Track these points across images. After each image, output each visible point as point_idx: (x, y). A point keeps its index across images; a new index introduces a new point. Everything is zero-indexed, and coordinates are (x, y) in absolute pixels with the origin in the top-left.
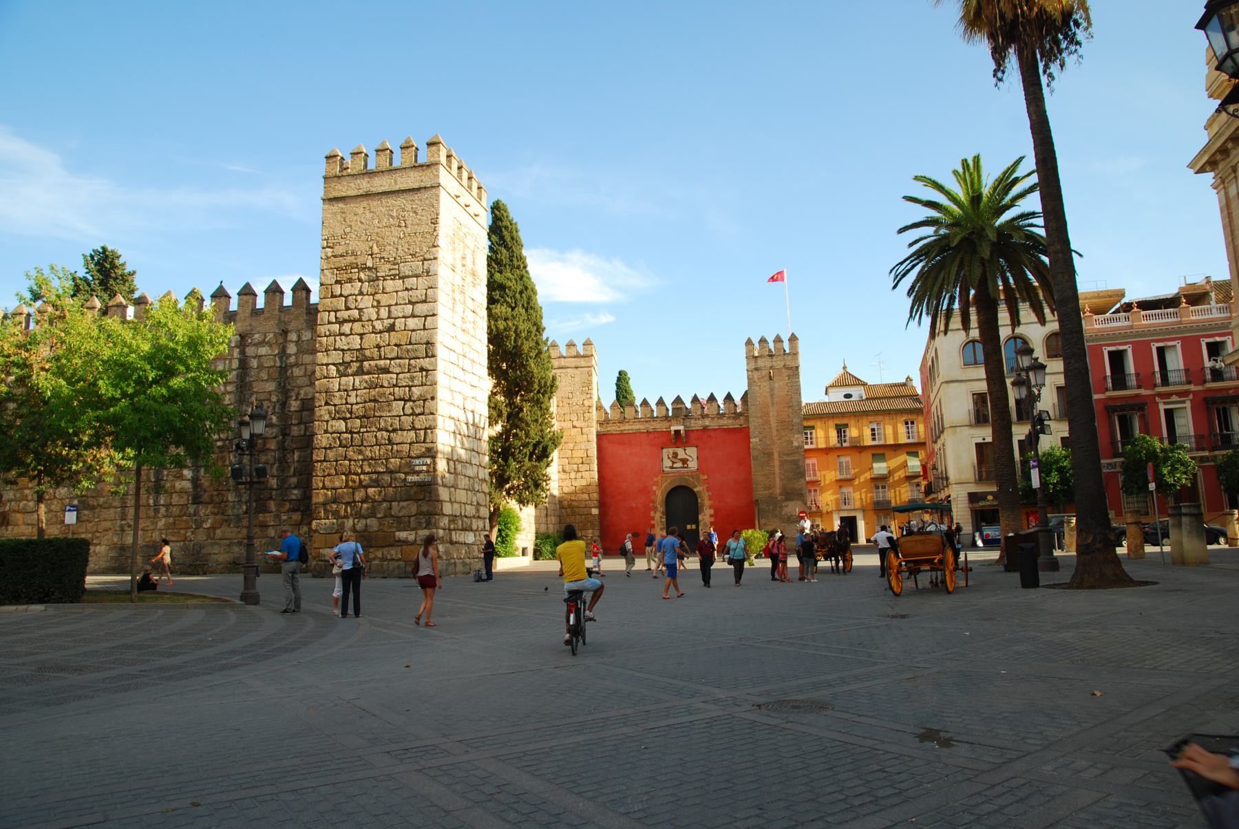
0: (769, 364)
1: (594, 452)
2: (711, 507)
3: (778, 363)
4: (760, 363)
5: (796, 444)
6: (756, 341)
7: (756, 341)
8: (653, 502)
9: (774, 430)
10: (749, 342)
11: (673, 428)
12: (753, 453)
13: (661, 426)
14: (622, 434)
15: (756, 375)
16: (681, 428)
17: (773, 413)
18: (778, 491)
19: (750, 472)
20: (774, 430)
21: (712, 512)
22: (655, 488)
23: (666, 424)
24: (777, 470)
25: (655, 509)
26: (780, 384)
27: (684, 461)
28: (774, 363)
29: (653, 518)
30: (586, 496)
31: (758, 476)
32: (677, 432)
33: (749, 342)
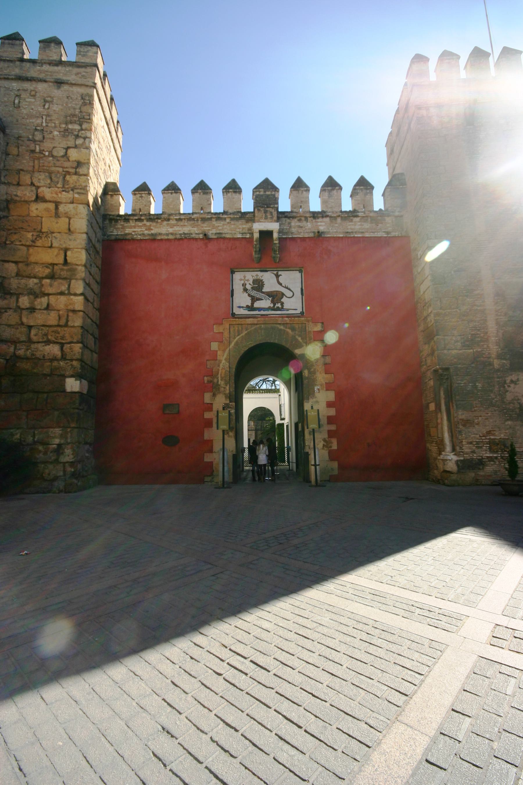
1: (79, 256)
2: (328, 387)
8: (212, 374)
14: (153, 239)
16: (274, 226)
18: (494, 349)
21: (331, 396)
22: (214, 346)
25: (214, 389)
27: (276, 297)
29: (209, 407)
30: (55, 350)
32: (266, 235)
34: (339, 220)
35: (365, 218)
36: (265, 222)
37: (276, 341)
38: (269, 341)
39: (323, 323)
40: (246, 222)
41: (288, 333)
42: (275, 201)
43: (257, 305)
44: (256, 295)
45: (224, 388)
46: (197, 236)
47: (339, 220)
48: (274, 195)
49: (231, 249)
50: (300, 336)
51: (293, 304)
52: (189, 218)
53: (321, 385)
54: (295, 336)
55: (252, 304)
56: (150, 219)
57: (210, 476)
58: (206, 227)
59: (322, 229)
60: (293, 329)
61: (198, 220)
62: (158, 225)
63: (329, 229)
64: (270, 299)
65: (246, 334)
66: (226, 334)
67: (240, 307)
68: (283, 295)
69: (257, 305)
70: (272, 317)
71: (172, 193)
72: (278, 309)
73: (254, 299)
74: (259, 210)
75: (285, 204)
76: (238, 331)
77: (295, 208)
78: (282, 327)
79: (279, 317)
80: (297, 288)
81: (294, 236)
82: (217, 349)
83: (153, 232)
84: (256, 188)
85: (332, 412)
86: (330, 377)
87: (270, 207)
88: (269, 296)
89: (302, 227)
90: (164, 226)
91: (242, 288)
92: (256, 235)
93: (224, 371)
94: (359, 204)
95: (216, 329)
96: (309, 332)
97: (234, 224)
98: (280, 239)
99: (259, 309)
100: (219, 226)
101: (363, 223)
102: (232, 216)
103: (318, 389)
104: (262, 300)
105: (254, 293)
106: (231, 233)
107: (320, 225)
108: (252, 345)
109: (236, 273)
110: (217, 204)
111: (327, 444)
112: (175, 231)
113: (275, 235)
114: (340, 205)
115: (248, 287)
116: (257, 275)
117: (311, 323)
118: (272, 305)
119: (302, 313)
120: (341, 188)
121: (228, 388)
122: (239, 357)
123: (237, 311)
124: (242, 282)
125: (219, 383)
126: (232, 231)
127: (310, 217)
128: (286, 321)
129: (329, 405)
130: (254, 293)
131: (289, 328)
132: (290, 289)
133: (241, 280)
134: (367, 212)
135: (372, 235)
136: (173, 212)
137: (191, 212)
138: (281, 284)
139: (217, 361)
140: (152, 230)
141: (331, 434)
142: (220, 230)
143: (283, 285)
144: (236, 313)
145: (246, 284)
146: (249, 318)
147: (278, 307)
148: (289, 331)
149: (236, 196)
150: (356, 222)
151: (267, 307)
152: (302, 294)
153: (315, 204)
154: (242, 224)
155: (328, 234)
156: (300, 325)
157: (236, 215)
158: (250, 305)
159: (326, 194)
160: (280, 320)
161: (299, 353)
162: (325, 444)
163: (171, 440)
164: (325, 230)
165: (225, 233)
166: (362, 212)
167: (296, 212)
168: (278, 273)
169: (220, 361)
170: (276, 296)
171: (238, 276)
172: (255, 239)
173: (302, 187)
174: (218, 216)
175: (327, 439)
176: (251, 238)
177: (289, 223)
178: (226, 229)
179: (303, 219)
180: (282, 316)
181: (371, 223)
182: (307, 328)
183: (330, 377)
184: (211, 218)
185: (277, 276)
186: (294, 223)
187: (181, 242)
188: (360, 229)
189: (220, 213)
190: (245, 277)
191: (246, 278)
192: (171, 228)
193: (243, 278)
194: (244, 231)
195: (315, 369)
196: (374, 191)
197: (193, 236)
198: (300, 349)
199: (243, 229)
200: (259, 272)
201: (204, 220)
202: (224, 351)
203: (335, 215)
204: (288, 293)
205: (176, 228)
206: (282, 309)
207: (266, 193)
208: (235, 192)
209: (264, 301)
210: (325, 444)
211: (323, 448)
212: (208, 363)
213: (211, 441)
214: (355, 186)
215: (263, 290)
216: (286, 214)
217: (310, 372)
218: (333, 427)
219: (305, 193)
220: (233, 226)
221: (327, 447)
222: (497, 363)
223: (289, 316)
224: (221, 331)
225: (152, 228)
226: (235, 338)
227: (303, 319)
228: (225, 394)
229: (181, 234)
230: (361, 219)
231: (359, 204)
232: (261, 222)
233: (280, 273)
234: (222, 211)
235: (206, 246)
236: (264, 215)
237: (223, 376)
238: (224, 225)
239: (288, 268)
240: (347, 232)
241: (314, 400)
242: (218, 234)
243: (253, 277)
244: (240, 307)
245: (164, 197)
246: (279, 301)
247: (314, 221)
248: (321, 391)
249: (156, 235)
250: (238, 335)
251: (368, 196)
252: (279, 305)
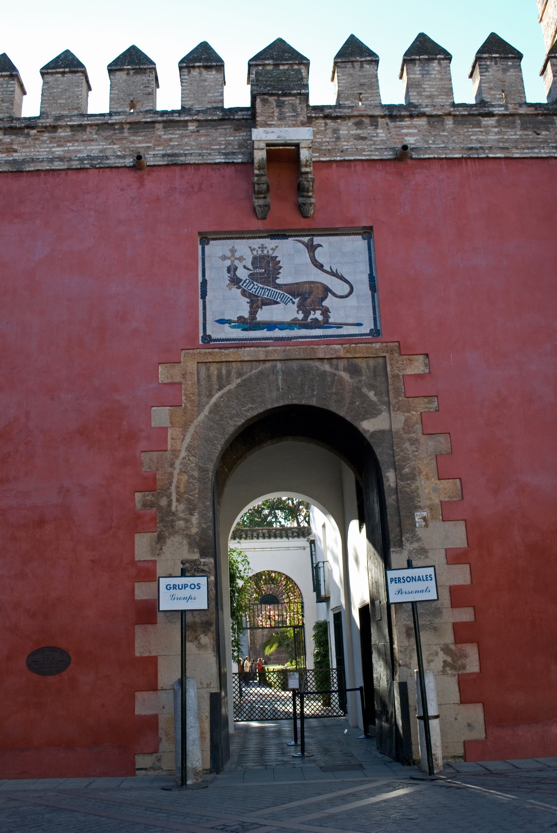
21: (456, 535)
22: (160, 416)
27: (310, 297)
34: (449, 123)
35: (507, 119)
36: (279, 126)
37: (314, 402)
38: (296, 402)
39: (427, 355)
40: (236, 130)
41: (341, 379)
42: (302, 85)
43: (263, 315)
44: (260, 293)
45: (187, 521)
46: (120, 162)
47: (449, 123)
48: (299, 72)
49: (200, 189)
50: (372, 387)
52: (103, 124)
53: (431, 508)
54: (359, 389)
55: (253, 313)
56: (11, 128)
57: (151, 753)
58: (140, 142)
59: (410, 141)
60: (354, 370)
61: (121, 129)
62: (29, 141)
63: (427, 142)
64: (296, 300)
65: (239, 385)
66: (190, 385)
67: (222, 322)
68: (327, 290)
69: (263, 315)
70: (302, 343)
71: (63, 73)
72: (316, 324)
73: (256, 303)
74: (265, 102)
75: (323, 89)
76: (219, 377)
77: (347, 99)
78: (327, 367)
79: (318, 344)
80: (360, 276)
81: (347, 158)
82: (168, 424)
83: (16, 156)
84: (257, 57)
85: (461, 576)
87: (290, 95)
88: (294, 295)
89: (364, 139)
90: (44, 142)
91: (227, 275)
92: (260, 155)
93: (185, 477)
94: (491, 89)
95: (164, 374)
96: (393, 376)
97: (206, 135)
99: (270, 326)
100: (171, 140)
101: (503, 130)
102: (201, 117)
103: (424, 519)
104: (276, 303)
105: (256, 288)
106: (200, 155)
107: (407, 135)
108: (255, 413)
109: (211, 242)
110: (169, 96)
111: (454, 664)
112: (69, 151)
113: (304, 154)
114: (449, 91)
115: (242, 274)
116: (263, 247)
117: (396, 355)
118: (300, 316)
119: (375, 332)
120: (448, 57)
121: (195, 519)
122: (223, 441)
124: (228, 263)
125: (173, 508)
126: (201, 148)
127: (383, 117)
128: (336, 351)
129: (455, 557)
130: (256, 288)
131: (345, 370)
132: (342, 278)
133: (224, 258)
134: (510, 106)
135: (528, 153)
136: (65, 113)
137: (107, 111)
138: (320, 267)
139: (168, 454)
140: (15, 151)
141: (462, 633)
142: (173, 147)
143: (327, 268)
144: (214, 336)
145: (236, 269)
146: (244, 346)
147: (316, 320)
148: (345, 376)
149: (212, 75)
150: (486, 127)
151: (288, 318)
152: (373, 288)
153: (392, 89)
154: (226, 135)
155: (426, 153)
156: (372, 362)
157: (211, 114)
158: (246, 315)
159: (417, 68)
160: (322, 351)
161: (372, 429)
162: (449, 659)
163: (48, 660)
164: (419, 145)
165: (185, 155)
166: (501, 106)
167: (350, 107)
168: (312, 240)
169: (175, 453)
170: (310, 293)
171: (216, 249)
172: (256, 165)
173: (361, 56)
174: (170, 120)
175: (452, 647)
177: (335, 131)
178: (187, 144)
179: (367, 121)
181: (524, 128)
182: (389, 369)
184: (154, 122)
185: (312, 248)
186: (346, 129)
187: (82, 175)
188: (498, 141)
189: (173, 112)
190: (233, 251)
191: (237, 255)
192: (59, 146)
193: (229, 254)
194: (230, 149)
195: (414, 469)
196: (524, 63)
197: (112, 162)
198: (373, 420)
199: (228, 143)
200: (268, 240)
201: (136, 126)
202: (185, 427)
203: (440, 113)
205: (71, 147)
206: (325, 324)
207: (279, 69)
208: (207, 68)
209: (282, 305)
210: (449, 659)
211: (444, 672)
212: (145, 457)
213: (153, 661)
214: (480, 52)
215: (278, 281)
216: (327, 111)
217: (400, 476)
218: (466, 615)
219: (367, 66)
220: (203, 139)
221: (453, 667)
224: (178, 379)
225: (15, 147)
226: (210, 396)
227: (378, 345)
228: (188, 536)
229: (81, 160)
230: (498, 121)
231: (491, 89)
232: (270, 126)
233: (317, 240)
234: (179, 108)
235: (142, 184)
236: (277, 110)
237: (182, 489)
238: (182, 136)
240: (471, 149)
241: (415, 545)
242: (169, 155)
243: (252, 250)
244: (222, 322)
245: (45, 83)
246: (318, 304)
247: (391, 124)
248: (430, 524)
249: (24, 161)
250: (219, 390)
251: (512, 72)
252: (318, 315)
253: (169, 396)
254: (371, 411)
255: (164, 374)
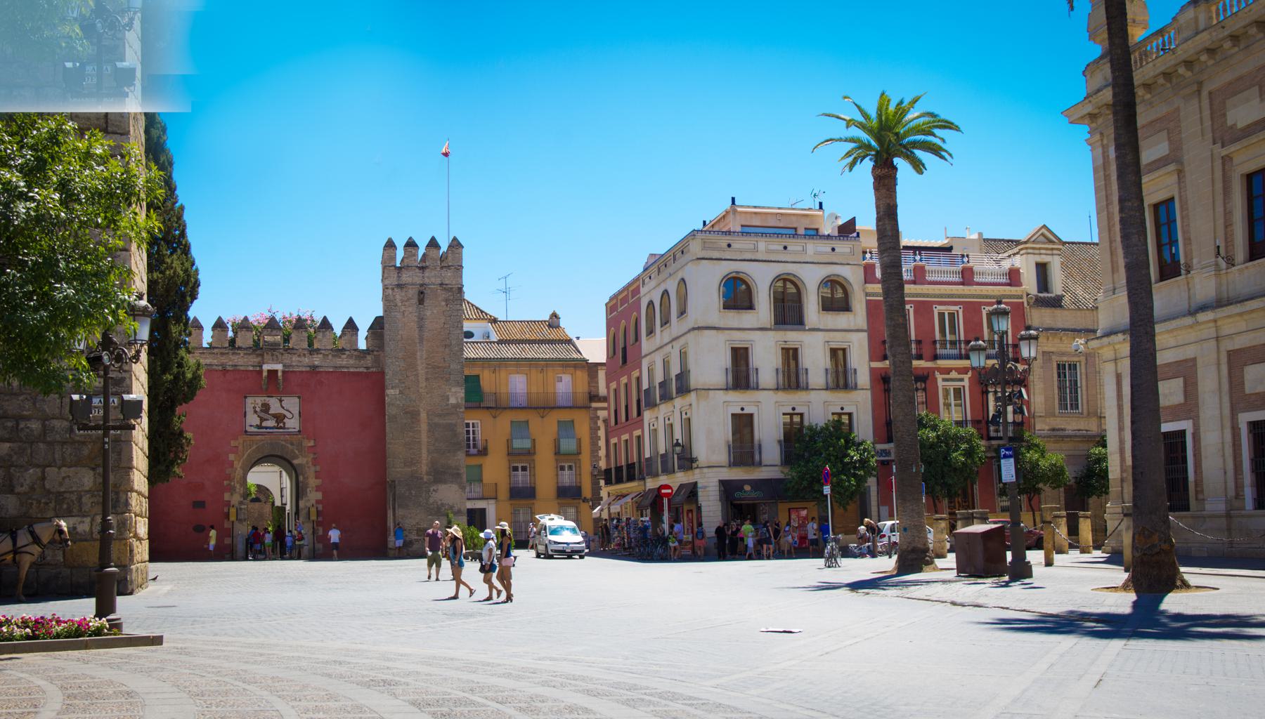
0: (418, 280)
2: (318, 489)
3: (432, 277)
4: (406, 277)
5: (452, 401)
6: (400, 244)
7: (400, 244)
8: (229, 478)
9: (422, 378)
10: (390, 245)
11: (266, 367)
12: (390, 411)
13: (244, 361)
15: (399, 295)
16: (279, 367)
17: (421, 355)
18: (424, 468)
19: (381, 438)
20: (422, 378)
21: (319, 496)
22: (232, 457)
23: (254, 360)
24: (424, 437)
26: (433, 310)
27: (280, 418)
28: (425, 277)
31: (396, 446)
32: (273, 373)
33: (390, 245)
35: (350, 357)
51: (293, 424)
60: (292, 444)
66: (240, 448)
69: (264, 424)
73: (262, 420)
80: (296, 411)
86: (319, 482)
92: (265, 374)
95: (233, 443)
98: (284, 372)
105: (262, 415)
113: (280, 374)
123: (249, 429)
129: (318, 502)
171: (250, 401)
176: (261, 372)
180: (284, 434)
183: (319, 482)
186: (295, 358)
204: (289, 415)
222: (425, 478)
223: (290, 434)
239: (290, 393)
253: (235, 450)
254: (297, 457)
255: (233, 443)
